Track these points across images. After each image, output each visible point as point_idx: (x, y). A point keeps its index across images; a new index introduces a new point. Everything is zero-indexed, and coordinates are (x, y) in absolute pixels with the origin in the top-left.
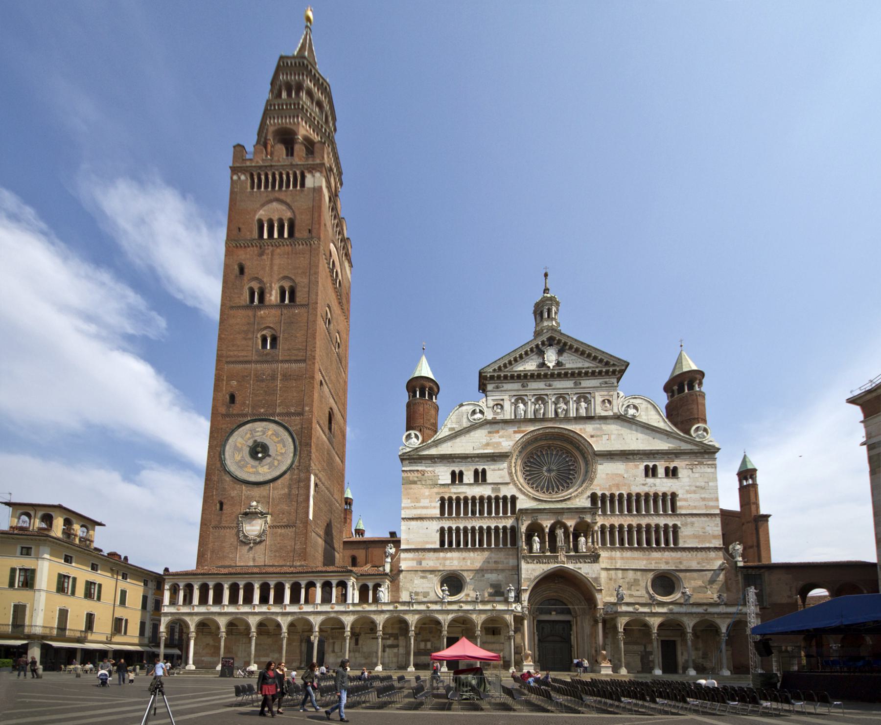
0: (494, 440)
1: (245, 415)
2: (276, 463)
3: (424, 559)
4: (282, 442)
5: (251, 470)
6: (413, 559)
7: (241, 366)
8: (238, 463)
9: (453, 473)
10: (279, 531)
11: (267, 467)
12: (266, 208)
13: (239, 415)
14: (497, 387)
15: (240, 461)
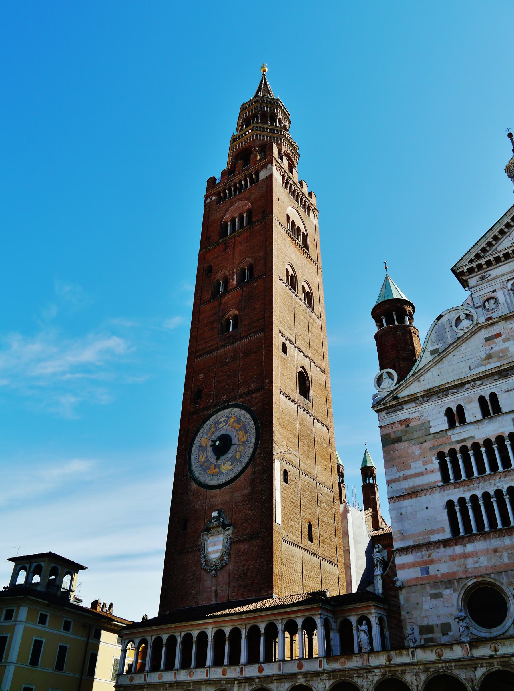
0: (496, 349)
1: (210, 407)
3: (432, 562)
4: (244, 429)
6: (414, 565)
7: (207, 356)
9: (449, 412)
11: (229, 463)
14: (483, 278)
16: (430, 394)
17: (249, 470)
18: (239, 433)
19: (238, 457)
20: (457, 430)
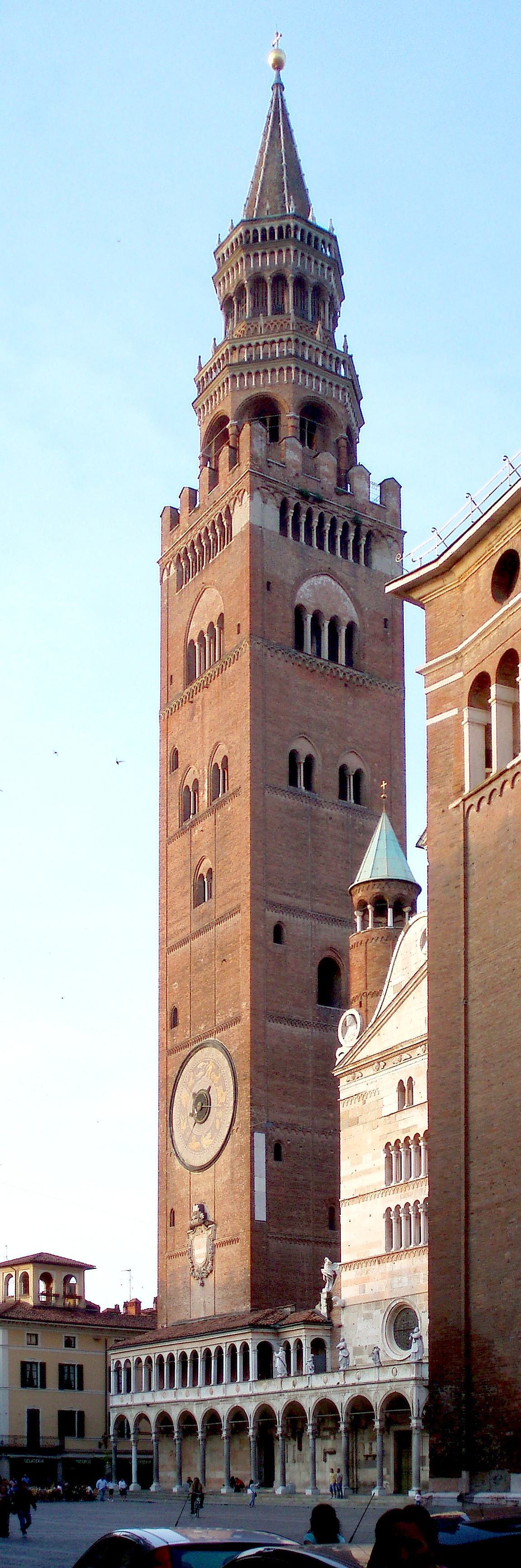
3: (367, 1280)
16: (383, 1059)
19: (218, 1127)
20: (405, 1114)
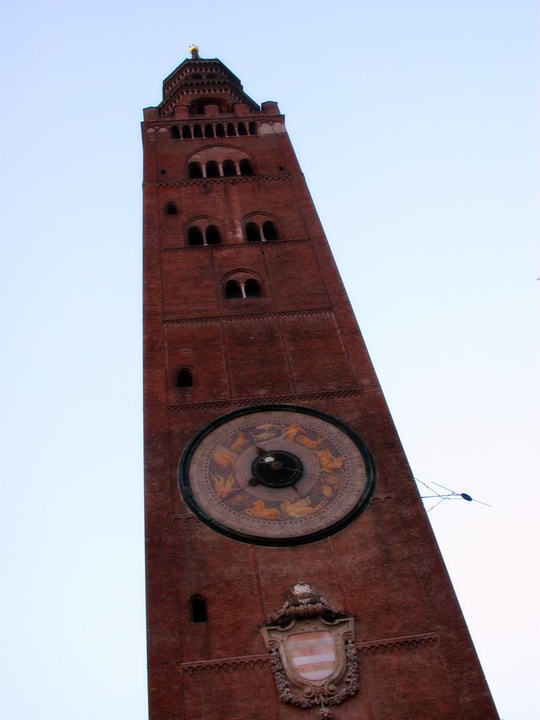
1: (227, 404)
2: (327, 492)
4: (328, 445)
5: (266, 512)
8: (226, 499)
10: (393, 660)
12: (202, 152)
13: (207, 405)
15: (231, 496)
17: (367, 517)
18: (319, 454)
